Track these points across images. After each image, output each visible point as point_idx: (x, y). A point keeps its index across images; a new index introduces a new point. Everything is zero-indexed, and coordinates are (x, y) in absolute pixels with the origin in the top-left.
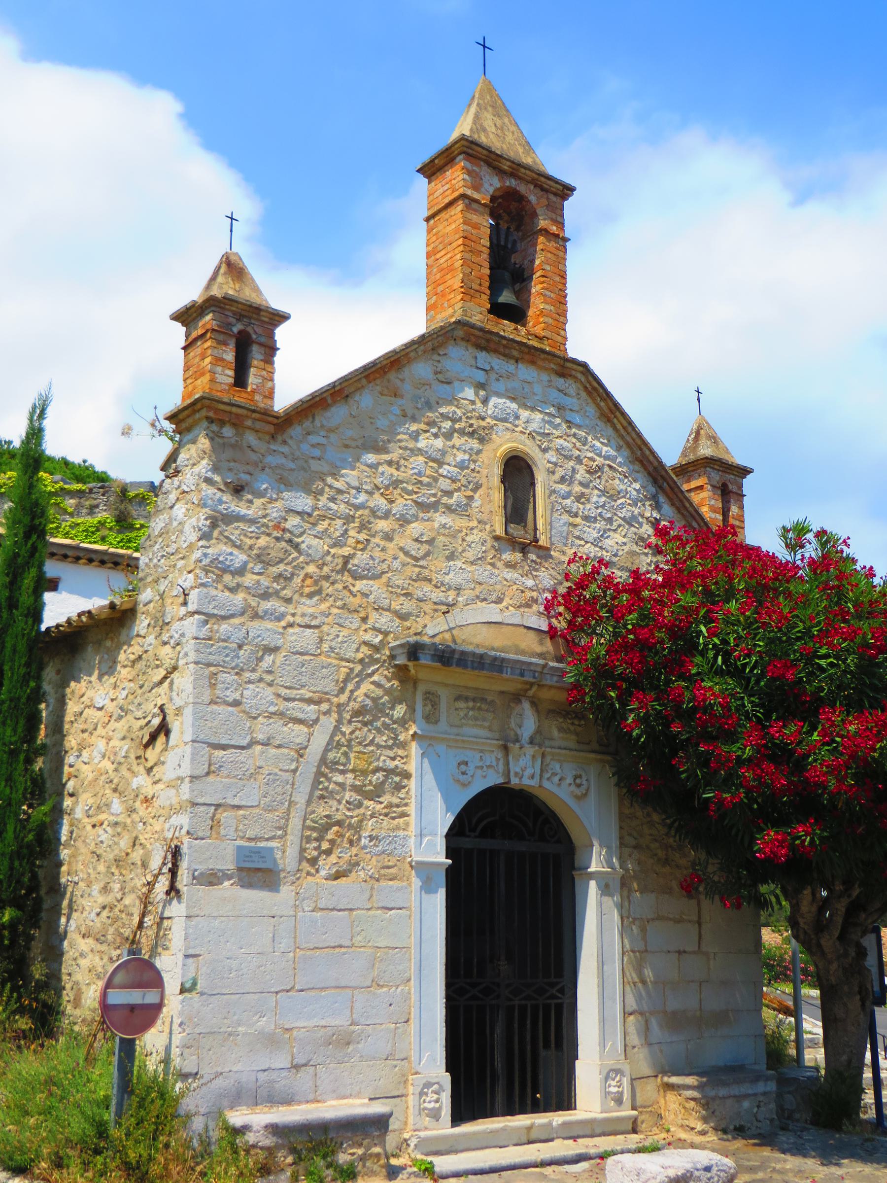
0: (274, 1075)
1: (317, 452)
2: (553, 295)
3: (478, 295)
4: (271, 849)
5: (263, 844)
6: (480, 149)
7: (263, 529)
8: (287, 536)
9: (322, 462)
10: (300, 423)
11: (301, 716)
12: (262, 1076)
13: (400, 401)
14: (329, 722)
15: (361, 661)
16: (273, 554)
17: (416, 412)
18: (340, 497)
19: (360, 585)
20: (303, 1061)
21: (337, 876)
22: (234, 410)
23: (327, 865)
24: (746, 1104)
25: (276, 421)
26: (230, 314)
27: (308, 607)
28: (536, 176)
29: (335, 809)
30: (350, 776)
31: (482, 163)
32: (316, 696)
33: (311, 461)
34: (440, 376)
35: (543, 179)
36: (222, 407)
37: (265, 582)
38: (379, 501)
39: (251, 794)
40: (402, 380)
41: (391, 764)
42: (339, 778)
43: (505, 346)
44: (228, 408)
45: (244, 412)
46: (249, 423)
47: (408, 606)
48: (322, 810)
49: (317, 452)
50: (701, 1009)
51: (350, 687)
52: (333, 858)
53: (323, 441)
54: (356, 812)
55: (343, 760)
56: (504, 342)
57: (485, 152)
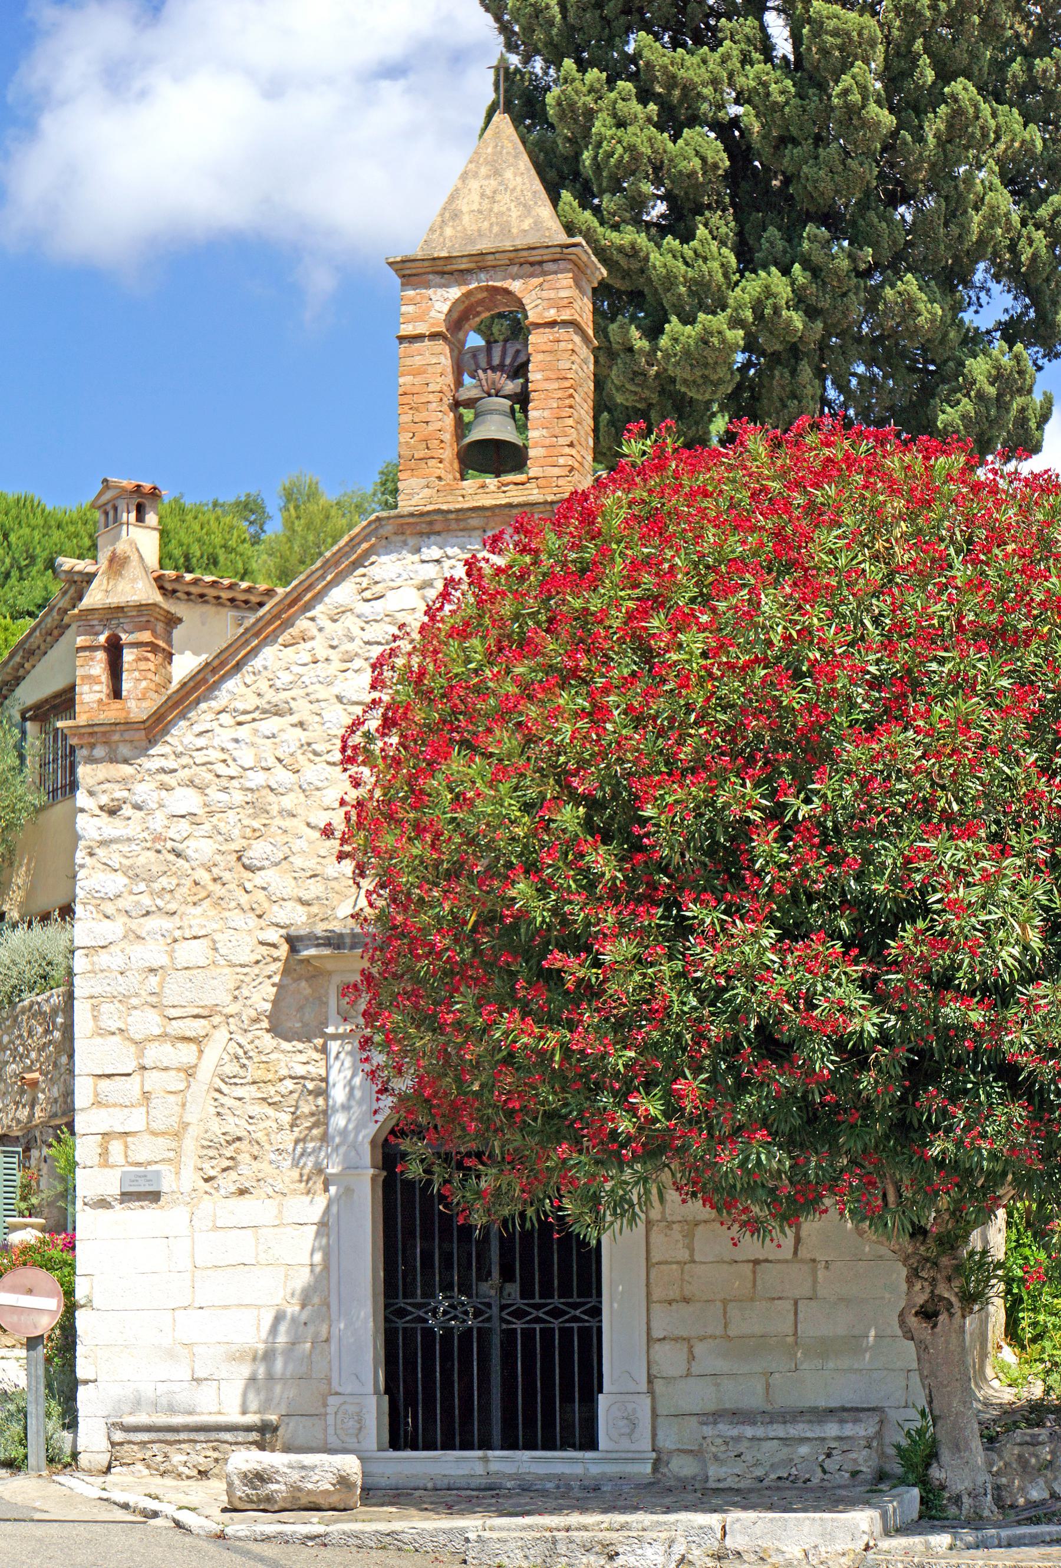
0: (175, 1387)
1: (201, 742)
2: (546, 414)
3: (422, 464)
4: (158, 1173)
5: (155, 1167)
6: (417, 264)
7: (144, 844)
8: (170, 844)
9: (210, 751)
10: (183, 716)
11: (188, 1034)
12: (162, 1388)
13: (309, 645)
14: (221, 1035)
15: (257, 962)
16: (154, 869)
17: (331, 651)
18: (235, 783)
19: (259, 879)
20: (205, 1376)
21: (242, 1192)
22: (96, 729)
23: (228, 1182)
24: (804, 1450)
25: (142, 726)
26: (95, 622)
27: (198, 919)
28: (512, 255)
29: (234, 1126)
30: (254, 1088)
31: (431, 277)
32: (205, 1013)
33: (195, 754)
34: (367, 594)
35: (525, 253)
36: (83, 730)
37: (146, 901)
38: (281, 776)
39: (136, 1121)
40: (313, 619)
41: (301, 1070)
42: (239, 1092)
43: (457, 520)
44: (90, 730)
45: (108, 728)
46: (116, 737)
47: (314, 889)
48: (216, 1127)
49: (201, 742)
50: (795, 1334)
51: (245, 992)
52: (233, 1175)
53: (207, 726)
54: (262, 1125)
55: (242, 1072)
56: (452, 516)
57: (426, 264)
